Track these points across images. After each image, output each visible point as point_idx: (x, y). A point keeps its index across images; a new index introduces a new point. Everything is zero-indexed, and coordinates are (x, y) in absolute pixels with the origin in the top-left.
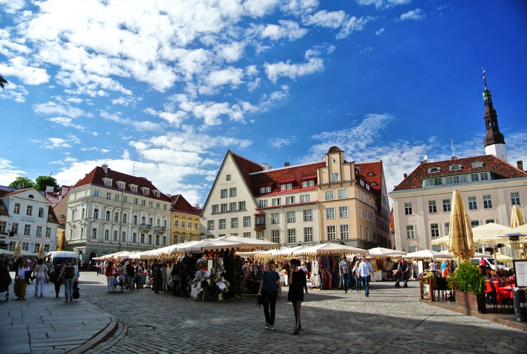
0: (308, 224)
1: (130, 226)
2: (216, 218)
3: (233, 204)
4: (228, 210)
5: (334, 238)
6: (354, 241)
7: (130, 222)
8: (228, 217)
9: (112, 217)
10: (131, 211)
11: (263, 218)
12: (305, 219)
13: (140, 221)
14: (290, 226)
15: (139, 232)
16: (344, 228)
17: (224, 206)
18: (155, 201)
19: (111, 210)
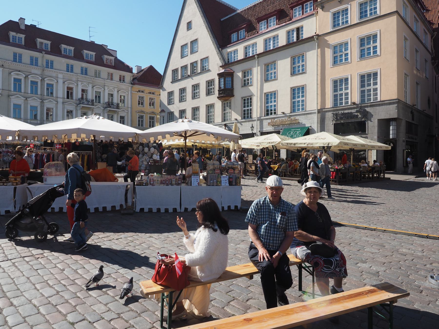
0: (298, 81)
1: (60, 101)
2: (176, 88)
3: (194, 65)
4: (189, 74)
5: (347, 103)
6: (390, 104)
7: (60, 94)
8: (188, 84)
9: (26, 87)
10: (61, 81)
11: (229, 79)
12: (293, 73)
13: (77, 94)
14: (269, 87)
15: (77, 110)
16: (367, 79)
17: (184, 68)
18: (105, 71)
19: (22, 77)
